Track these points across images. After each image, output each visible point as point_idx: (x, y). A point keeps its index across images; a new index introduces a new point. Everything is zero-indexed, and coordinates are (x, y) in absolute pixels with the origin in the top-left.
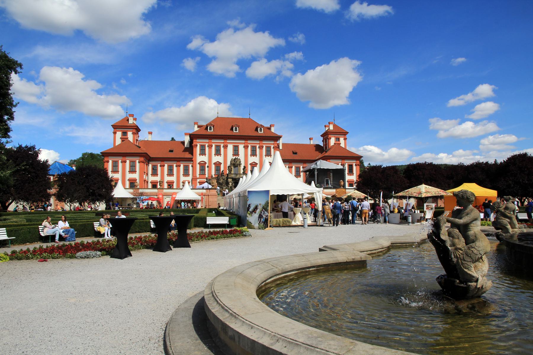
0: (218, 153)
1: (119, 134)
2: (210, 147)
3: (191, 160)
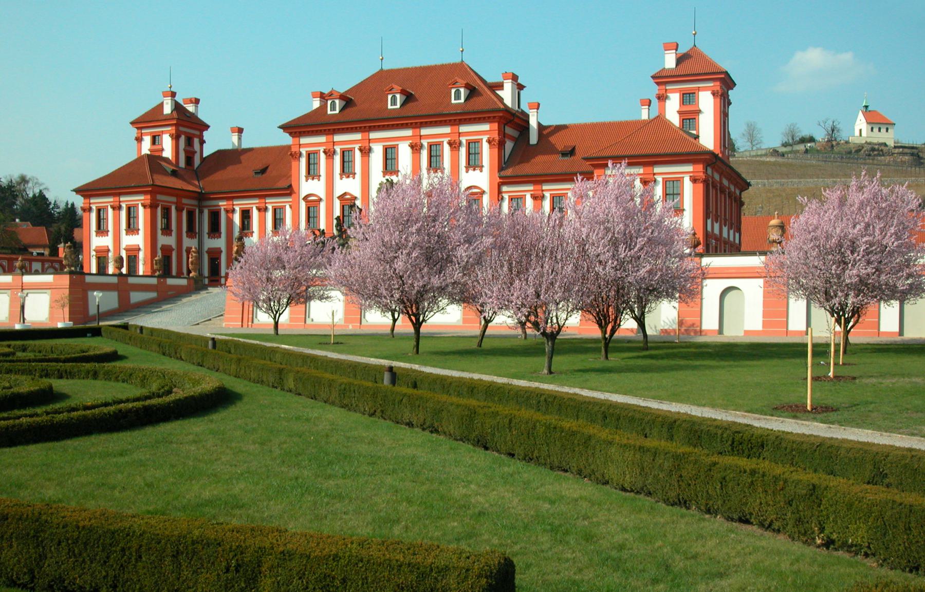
0: (347, 171)
1: (147, 140)
2: (330, 154)
3: (289, 191)
